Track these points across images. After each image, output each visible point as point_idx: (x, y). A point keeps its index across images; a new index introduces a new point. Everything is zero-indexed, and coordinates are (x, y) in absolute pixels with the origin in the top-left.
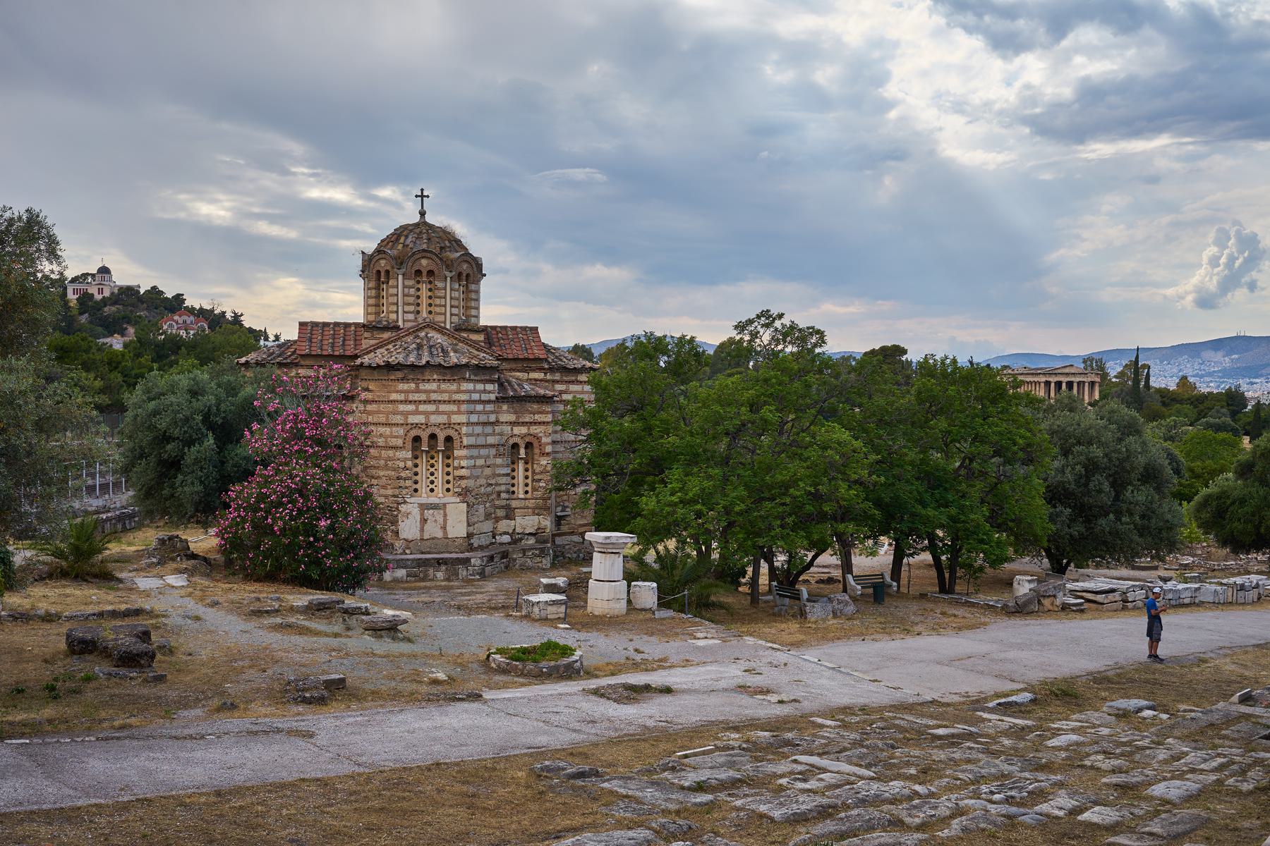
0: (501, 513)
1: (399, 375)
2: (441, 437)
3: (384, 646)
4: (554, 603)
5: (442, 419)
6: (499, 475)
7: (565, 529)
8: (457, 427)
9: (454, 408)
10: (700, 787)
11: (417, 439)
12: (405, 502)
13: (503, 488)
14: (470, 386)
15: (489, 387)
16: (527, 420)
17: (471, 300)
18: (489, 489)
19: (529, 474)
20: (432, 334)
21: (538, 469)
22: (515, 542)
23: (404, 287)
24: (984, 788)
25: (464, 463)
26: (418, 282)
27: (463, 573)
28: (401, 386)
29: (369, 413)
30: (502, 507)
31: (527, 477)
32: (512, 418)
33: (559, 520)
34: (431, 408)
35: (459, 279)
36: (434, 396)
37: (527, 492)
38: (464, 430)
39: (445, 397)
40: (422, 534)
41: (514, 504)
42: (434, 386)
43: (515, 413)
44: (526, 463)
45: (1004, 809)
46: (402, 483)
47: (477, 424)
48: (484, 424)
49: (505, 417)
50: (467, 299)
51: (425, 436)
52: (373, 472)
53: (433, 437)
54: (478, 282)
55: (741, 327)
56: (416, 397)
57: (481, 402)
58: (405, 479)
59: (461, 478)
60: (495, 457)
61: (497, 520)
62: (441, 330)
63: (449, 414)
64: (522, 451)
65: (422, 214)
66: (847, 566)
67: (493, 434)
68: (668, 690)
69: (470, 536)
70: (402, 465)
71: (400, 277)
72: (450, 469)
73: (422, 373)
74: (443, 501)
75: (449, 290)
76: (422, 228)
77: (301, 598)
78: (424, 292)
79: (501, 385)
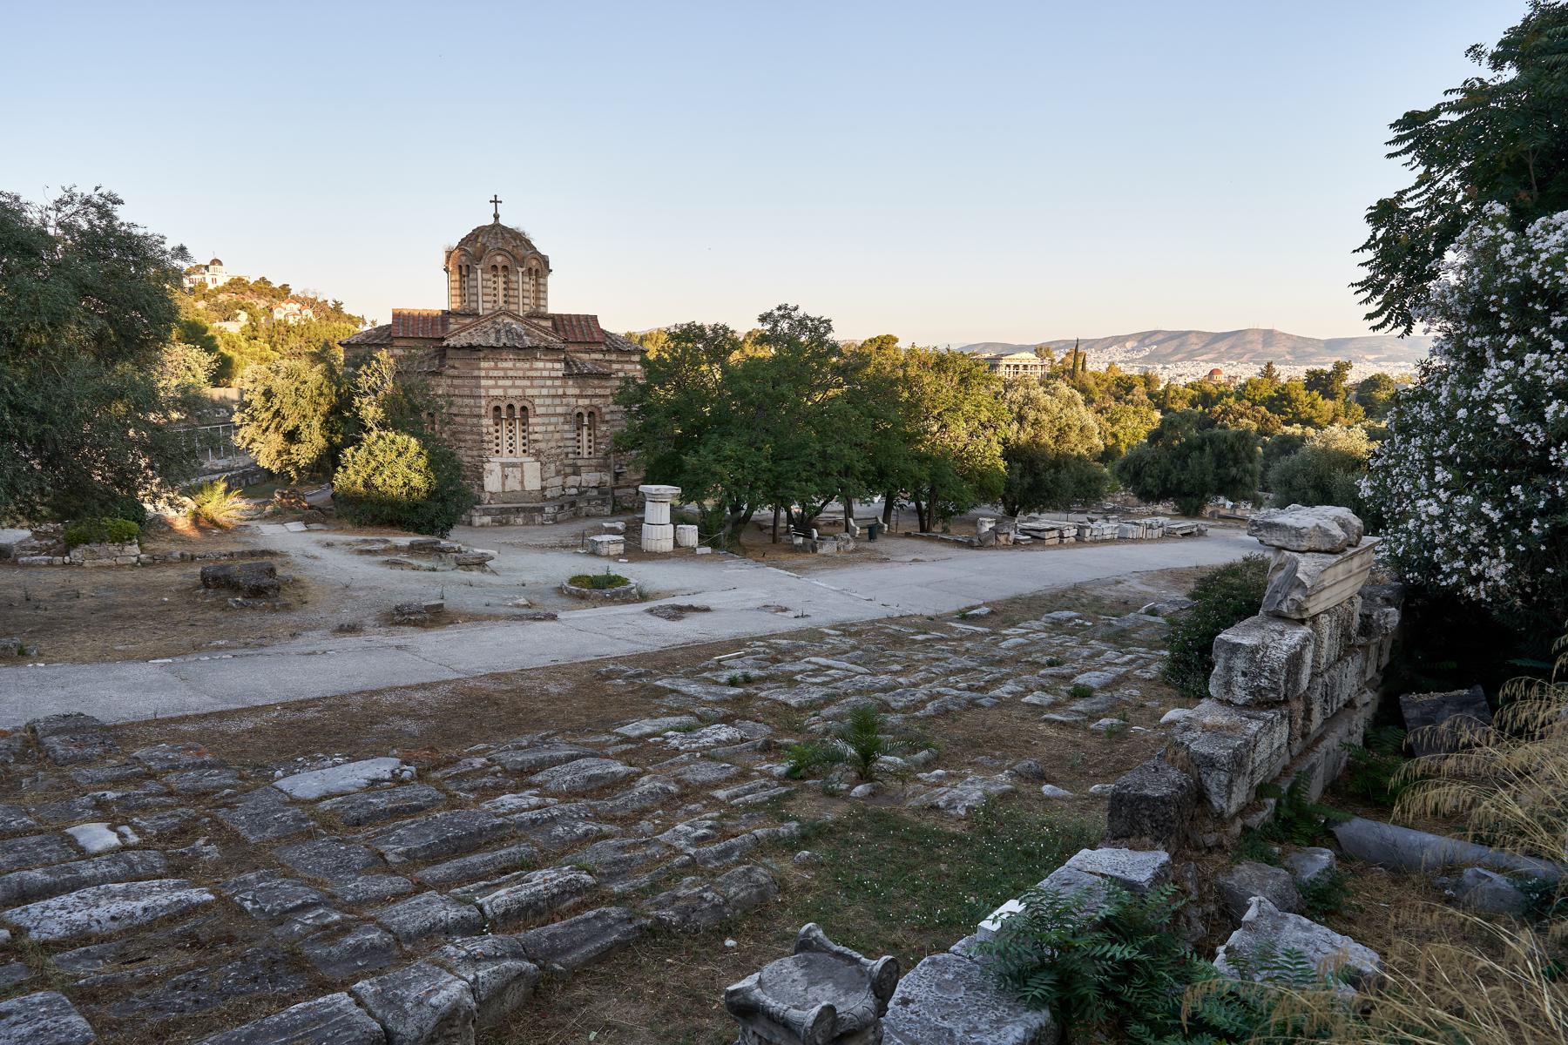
0: (569, 470)
1: (482, 355)
2: (517, 407)
3: (475, 575)
4: (615, 542)
5: (518, 392)
7: (622, 483)
9: (527, 383)
10: (733, 683)
11: (497, 409)
14: (540, 365)
15: (557, 366)
17: (540, 292)
20: (508, 320)
22: (580, 494)
24: (951, 679)
25: (537, 429)
27: (538, 519)
28: (483, 364)
29: (455, 387)
32: (577, 391)
33: (617, 476)
34: (508, 383)
36: (510, 373)
38: (537, 401)
39: (520, 374)
41: (580, 462)
42: (510, 364)
45: (967, 694)
49: (570, 391)
50: (538, 291)
51: (504, 406)
53: (511, 406)
54: (545, 277)
55: (763, 319)
56: (495, 373)
57: (550, 378)
59: (536, 441)
61: (566, 475)
62: (515, 317)
63: (524, 388)
65: (496, 217)
66: (848, 512)
68: (707, 610)
69: (543, 489)
75: (522, 283)
76: (496, 230)
77: (404, 540)
78: (501, 286)
79: (567, 364)
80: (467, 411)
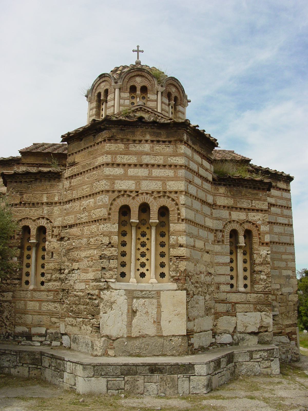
0: (221, 308)
6: (219, 264)
8: (173, 196)
9: (169, 173)
12: (108, 288)
13: (222, 279)
16: (245, 205)
18: (208, 279)
19: (248, 265)
21: (258, 260)
23: (120, 98)
25: (182, 240)
26: (133, 98)
27: (184, 385)
30: (223, 301)
31: (245, 270)
32: (229, 202)
35: (170, 100)
36: (146, 159)
37: (245, 286)
39: (160, 160)
40: (129, 331)
43: (233, 196)
44: (244, 254)
46: (105, 263)
47: (196, 198)
48: (204, 202)
49: (222, 201)
52: (74, 254)
56: (125, 159)
58: (109, 258)
59: (180, 258)
60: (214, 242)
61: (217, 315)
63: (164, 180)
64: (242, 240)
67: (211, 216)
69: (190, 334)
70: (106, 240)
71: (117, 91)
72: (165, 250)
73: (133, 133)
74: (158, 286)
80: (84, 217)
